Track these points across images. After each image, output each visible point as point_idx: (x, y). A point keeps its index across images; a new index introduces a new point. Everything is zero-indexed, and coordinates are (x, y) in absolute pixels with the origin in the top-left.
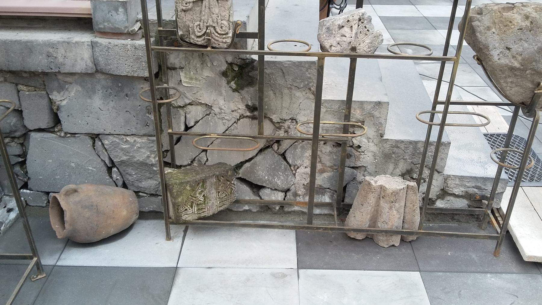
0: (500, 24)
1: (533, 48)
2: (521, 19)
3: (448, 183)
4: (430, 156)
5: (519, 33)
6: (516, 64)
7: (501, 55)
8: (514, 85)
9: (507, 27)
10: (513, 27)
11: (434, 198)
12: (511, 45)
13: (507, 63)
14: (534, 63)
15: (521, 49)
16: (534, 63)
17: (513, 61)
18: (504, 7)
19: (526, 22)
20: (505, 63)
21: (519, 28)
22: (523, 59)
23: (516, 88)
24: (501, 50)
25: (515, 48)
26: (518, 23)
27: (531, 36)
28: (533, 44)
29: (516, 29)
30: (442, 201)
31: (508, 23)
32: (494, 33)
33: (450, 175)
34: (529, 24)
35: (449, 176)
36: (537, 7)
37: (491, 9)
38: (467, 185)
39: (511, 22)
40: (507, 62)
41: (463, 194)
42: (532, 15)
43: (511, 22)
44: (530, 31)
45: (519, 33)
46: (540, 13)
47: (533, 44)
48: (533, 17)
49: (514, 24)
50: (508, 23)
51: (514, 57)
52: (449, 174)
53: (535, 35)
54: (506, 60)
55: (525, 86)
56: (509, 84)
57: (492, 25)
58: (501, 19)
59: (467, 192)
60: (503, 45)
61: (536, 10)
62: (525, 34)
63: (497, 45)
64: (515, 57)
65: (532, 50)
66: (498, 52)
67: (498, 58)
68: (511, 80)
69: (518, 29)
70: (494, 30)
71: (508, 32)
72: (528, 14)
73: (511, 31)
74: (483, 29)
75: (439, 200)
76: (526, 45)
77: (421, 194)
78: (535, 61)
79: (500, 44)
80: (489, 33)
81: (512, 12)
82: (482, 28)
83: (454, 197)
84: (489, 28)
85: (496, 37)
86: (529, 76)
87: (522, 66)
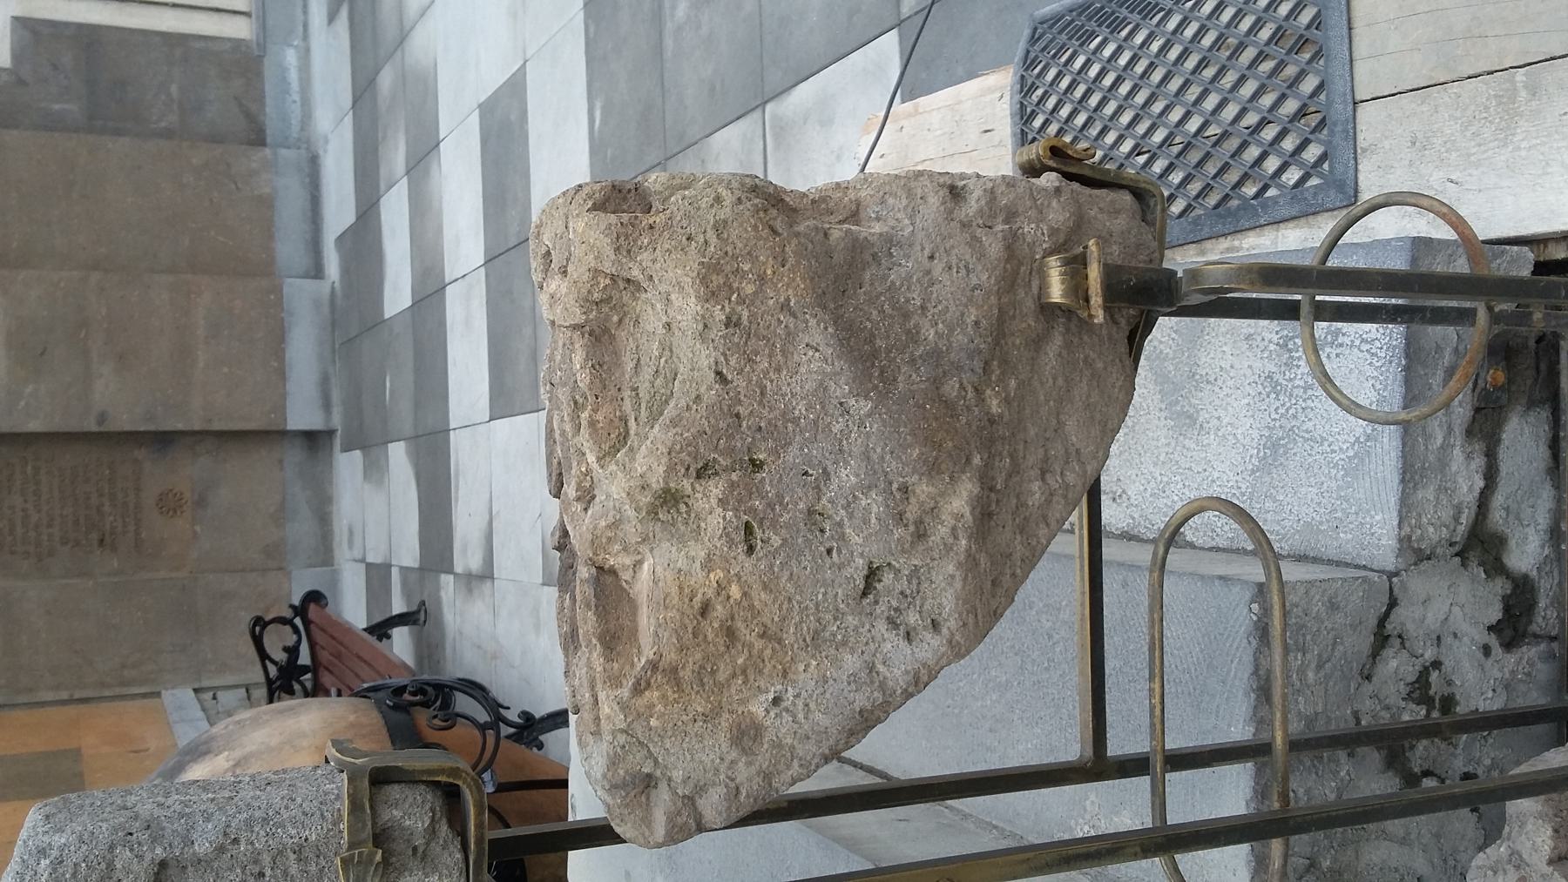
0: (722, 676)
1: (861, 424)
2: (682, 541)
3: (1435, 538)
4: (1322, 674)
5: (776, 541)
6: (959, 502)
7: (912, 618)
8: (1056, 450)
9: (740, 624)
10: (735, 591)
11: (1501, 586)
12: (848, 572)
13: (959, 565)
14: (951, 388)
15: (874, 504)
16: (951, 388)
17: (943, 531)
18: (601, 639)
19: (700, 504)
20: (958, 584)
21: (742, 548)
22: (932, 469)
23: (1071, 425)
24: (881, 626)
25: (861, 547)
26: (708, 565)
27: (792, 455)
28: (836, 428)
29: (748, 563)
30: (1512, 543)
31: (711, 628)
32: (776, 701)
33: (1400, 540)
34: (716, 488)
35: (1405, 542)
36: (592, 424)
37: (622, 738)
38: (1439, 441)
39: (705, 610)
40: (951, 568)
41: (1479, 446)
42: (657, 482)
43: (705, 610)
44: (757, 466)
45: (776, 541)
46: (627, 393)
47: (836, 428)
48: (671, 469)
49: (720, 587)
50: (711, 628)
51: (921, 535)
52: (1393, 543)
53: (778, 432)
54: (939, 579)
55: (1060, 381)
56: (1054, 481)
57: (725, 720)
58: (686, 674)
59: (1469, 433)
60: (851, 620)
61: (615, 440)
62: (780, 497)
63: (851, 662)
64: (919, 523)
65: (873, 427)
66: (892, 644)
67: (928, 636)
68: (1036, 486)
69: (751, 550)
70: (758, 708)
71: (771, 615)
72: (646, 499)
73: (760, 597)
74: (749, 764)
75: (1506, 560)
76: (847, 476)
77: (1490, 661)
78: (937, 383)
79: (844, 643)
80: (779, 727)
81: (626, 576)
82: (743, 773)
83: (1493, 492)
84: (746, 735)
85: (806, 674)
86: (1013, 383)
87: (968, 460)
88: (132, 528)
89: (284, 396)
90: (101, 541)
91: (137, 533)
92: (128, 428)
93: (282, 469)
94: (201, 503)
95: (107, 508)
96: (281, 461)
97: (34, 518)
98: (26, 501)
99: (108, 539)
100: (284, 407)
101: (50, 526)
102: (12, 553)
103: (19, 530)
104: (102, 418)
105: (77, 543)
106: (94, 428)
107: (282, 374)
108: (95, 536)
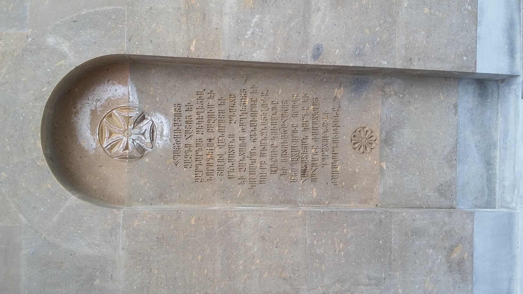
88: (330, 161)
89: (475, 39)
90: (304, 172)
91: (334, 167)
92: (340, 63)
93: (456, 113)
94: (387, 141)
95: (310, 142)
96: (456, 106)
97: (250, 146)
98: (243, 130)
99: (309, 172)
100: (474, 51)
101: (262, 155)
102: (230, 178)
103: (237, 158)
104: (318, 51)
105: (284, 173)
106: (311, 62)
107: (474, 17)
108: (299, 167)
